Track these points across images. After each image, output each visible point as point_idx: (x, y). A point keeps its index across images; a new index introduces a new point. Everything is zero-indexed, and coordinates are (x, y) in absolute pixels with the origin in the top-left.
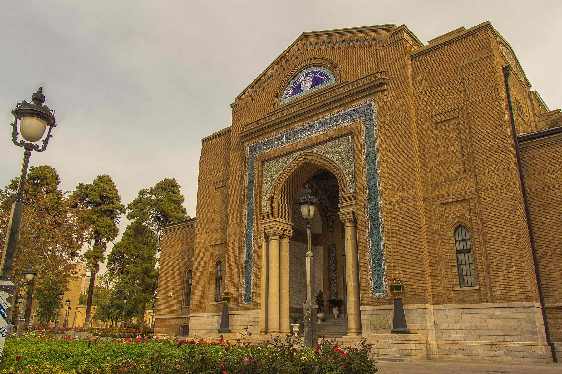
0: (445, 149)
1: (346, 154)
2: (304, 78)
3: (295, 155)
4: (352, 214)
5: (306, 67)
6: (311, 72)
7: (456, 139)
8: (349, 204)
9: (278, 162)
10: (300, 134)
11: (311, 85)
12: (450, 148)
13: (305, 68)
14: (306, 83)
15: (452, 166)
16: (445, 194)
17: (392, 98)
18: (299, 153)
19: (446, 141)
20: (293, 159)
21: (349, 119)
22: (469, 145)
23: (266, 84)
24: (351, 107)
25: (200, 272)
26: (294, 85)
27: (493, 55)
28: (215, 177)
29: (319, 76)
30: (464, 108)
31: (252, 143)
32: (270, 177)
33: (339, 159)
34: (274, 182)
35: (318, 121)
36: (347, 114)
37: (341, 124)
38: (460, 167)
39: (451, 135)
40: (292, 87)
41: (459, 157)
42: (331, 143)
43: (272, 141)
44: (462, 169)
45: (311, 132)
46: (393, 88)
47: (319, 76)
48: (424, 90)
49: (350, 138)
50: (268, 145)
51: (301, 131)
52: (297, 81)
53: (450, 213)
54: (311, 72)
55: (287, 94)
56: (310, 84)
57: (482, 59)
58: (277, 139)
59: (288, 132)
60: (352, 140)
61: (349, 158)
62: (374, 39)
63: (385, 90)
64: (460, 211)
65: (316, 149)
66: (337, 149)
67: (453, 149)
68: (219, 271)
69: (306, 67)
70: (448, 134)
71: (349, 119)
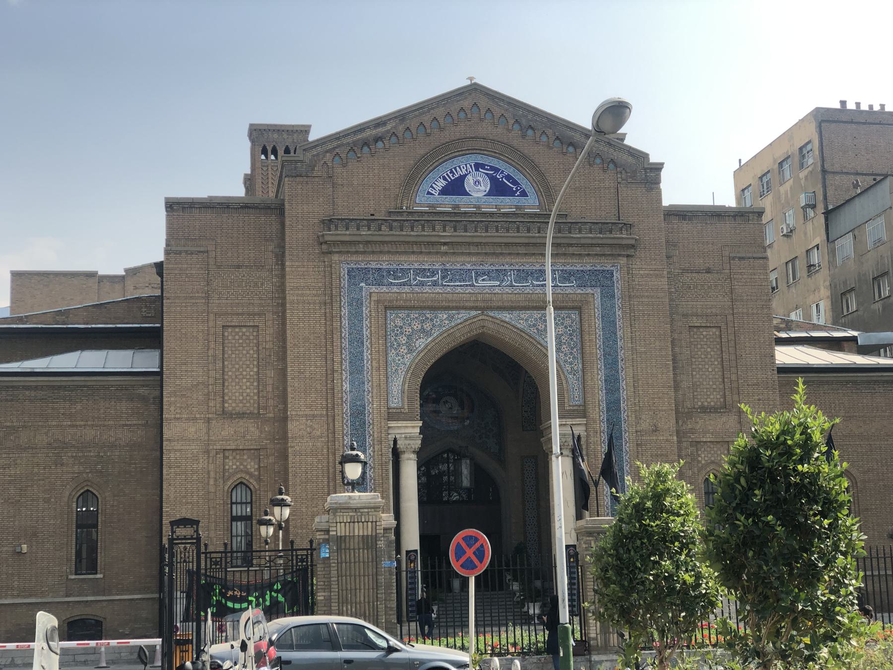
0: (700, 366)
1: (566, 340)
2: (470, 170)
3: (463, 315)
5: (478, 151)
6: (488, 166)
7: (716, 356)
9: (422, 317)
10: (476, 280)
11: (487, 190)
12: (707, 366)
13: (475, 151)
14: (477, 183)
15: (709, 393)
16: (699, 429)
17: (641, 272)
18: (473, 313)
19: (703, 356)
20: (459, 321)
21: (573, 283)
22: (733, 370)
23: (380, 144)
24: (579, 263)
25: (188, 503)
26: (447, 174)
27: (766, 258)
28: (219, 299)
29: (504, 179)
30: (730, 318)
31: (357, 262)
32: (404, 342)
34: (414, 354)
35: (512, 267)
37: (557, 286)
38: (718, 397)
39: (709, 350)
40: (445, 179)
41: (718, 383)
42: (539, 314)
43: (410, 272)
44: (722, 400)
45: (499, 283)
46: (643, 255)
47: (504, 179)
48: (677, 271)
49: (574, 315)
50: (399, 278)
51: (478, 275)
52: (455, 168)
53: (703, 456)
54: (488, 166)
55: (432, 186)
56: (486, 188)
57: (754, 258)
59: (448, 266)
60: (578, 319)
61: (572, 348)
62: (612, 161)
64: (716, 455)
65: (508, 316)
67: (710, 370)
68: (234, 503)
69: (478, 151)
70: (705, 346)
71: (573, 283)
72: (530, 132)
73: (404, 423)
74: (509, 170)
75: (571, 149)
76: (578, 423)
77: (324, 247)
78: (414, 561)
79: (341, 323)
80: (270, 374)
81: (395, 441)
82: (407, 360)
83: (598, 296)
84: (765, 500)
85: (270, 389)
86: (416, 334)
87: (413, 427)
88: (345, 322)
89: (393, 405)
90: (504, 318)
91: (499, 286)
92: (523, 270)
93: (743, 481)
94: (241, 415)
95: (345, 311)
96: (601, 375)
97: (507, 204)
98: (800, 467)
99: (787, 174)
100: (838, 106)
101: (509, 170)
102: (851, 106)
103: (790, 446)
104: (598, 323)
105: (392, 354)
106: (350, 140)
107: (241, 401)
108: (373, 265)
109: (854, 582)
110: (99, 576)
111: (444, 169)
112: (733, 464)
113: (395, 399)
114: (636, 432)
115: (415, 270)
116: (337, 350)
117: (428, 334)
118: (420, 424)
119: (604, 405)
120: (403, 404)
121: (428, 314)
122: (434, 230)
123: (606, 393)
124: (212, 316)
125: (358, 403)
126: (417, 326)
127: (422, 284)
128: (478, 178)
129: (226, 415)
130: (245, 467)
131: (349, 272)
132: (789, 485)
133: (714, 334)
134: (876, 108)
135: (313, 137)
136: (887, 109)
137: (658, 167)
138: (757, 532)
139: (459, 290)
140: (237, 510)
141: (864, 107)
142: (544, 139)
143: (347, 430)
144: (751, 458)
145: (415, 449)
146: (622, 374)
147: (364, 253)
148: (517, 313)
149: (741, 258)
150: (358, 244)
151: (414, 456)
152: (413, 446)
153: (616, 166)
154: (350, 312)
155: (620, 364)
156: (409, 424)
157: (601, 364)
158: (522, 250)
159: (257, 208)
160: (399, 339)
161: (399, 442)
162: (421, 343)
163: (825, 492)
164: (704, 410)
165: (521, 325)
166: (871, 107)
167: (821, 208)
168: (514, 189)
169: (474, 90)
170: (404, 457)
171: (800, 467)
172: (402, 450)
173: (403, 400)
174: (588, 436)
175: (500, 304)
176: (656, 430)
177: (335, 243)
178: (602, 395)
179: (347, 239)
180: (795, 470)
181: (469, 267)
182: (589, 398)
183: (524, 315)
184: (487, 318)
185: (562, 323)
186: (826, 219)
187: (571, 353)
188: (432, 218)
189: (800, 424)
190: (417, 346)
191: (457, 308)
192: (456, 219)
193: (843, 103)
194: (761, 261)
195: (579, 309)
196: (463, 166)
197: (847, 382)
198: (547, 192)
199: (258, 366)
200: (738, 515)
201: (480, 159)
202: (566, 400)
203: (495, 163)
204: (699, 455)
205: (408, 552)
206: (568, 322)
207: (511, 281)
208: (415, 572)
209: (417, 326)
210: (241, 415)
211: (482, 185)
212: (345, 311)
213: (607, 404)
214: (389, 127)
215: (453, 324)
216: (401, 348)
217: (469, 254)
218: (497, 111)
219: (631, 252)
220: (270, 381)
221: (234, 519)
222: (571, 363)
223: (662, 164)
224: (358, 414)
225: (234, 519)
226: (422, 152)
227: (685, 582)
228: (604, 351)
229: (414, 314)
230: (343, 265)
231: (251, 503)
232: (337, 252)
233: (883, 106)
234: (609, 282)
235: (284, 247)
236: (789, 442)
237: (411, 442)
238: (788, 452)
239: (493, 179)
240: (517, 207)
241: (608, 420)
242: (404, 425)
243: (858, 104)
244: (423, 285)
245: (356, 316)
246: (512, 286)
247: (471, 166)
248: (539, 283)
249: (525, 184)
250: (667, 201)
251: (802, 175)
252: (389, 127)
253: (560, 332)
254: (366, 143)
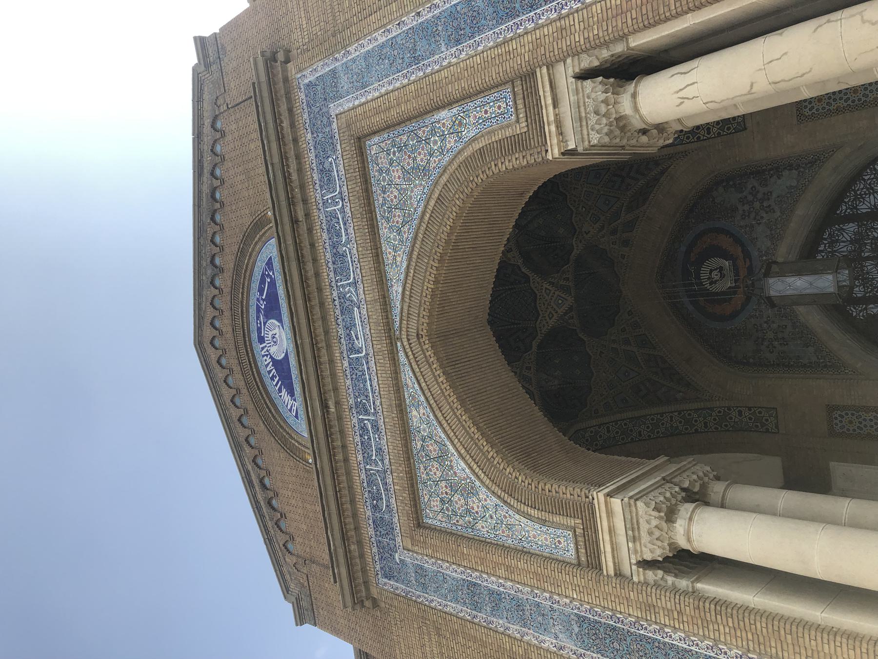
3: (407, 376)
4: (588, 83)
6: (257, 323)
8: (549, 101)
11: (278, 324)
20: (416, 386)
21: (331, 163)
33: (421, 184)
34: (478, 483)
37: (340, 193)
47: (264, 297)
51: (353, 349)
58: (366, 446)
60: (376, 139)
63: (288, 52)
66: (395, 197)
76: (548, 88)
79: (451, 614)
81: (645, 564)
82: (488, 501)
86: (447, 474)
87: (610, 513)
89: (572, 552)
90: (399, 297)
91: (359, 308)
92: (334, 263)
113: (559, 542)
120: (567, 528)
121: (416, 444)
123: (480, 31)
125: (576, 629)
126: (436, 471)
128: (270, 336)
131: (386, 577)
137: (201, 43)
139: (375, 384)
145: (660, 518)
150: (350, 551)
152: (654, 522)
156: (603, 524)
160: (459, 509)
161: (648, 557)
162: (460, 467)
165: (402, 260)
168: (269, 280)
172: (668, 548)
173: (558, 526)
174: (576, 53)
181: (346, 364)
182: (494, 74)
184: (404, 329)
190: (464, 475)
195: (359, 138)
201: (254, 336)
202: (509, 132)
207: (349, 284)
211: (274, 332)
213: (500, 21)
215: (422, 398)
216: (473, 508)
219: (281, 57)
222: (443, 137)
223: (195, 38)
228: (410, 65)
232: (368, 589)
234: (319, 88)
237: (644, 527)
242: (607, 537)
244: (381, 449)
246: (355, 283)
247: (263, 348)
248: (343, 230)
252: (250, 468)
253: (400, 172)
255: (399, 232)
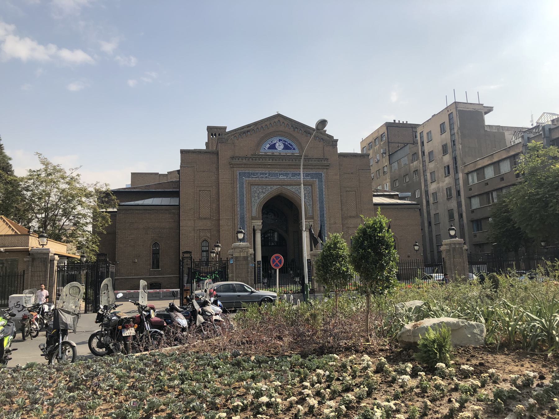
3: (275, 187)
18: (278, 187)
20: (274, 189)
23: (249, 133)
27: (370, 169)
31: (242, 170)
36: (309, 174)
40: (269, 144)
49: (310, 187)
68: (204, 246)
72: (296, 129)
73: (257, 221)
74: (289, 142)
75: (309, 135)
77: (231, 165)
78: (260, 264)
80: (214, 206)
81: (254, 226)
83: (317, 181)
84: (368, 245)
85: (214, 210)
87: (260, 222)
88: (238, 189)
93: (361, 239)
94: (205, 219)
95: (238, 186)
96: (318, 206)
97: (289, 152)
98: (379, 234)
99: (377, 143)
100: (393, 122)
101: (289, 142)
102: (397, 122)
103: (376, 228)
104: (317, 190)
105: (253, 199)
106: (239, 131)
107: (205, 214)
108: (247, 171)
109: (395, 270)
110: (160, 269)
111: (269, 141)
112: (358, 233)
114: (329, 224)
115: (260, 173)
116: (236, 198)
117: (264, 193)
118: (262, 221)
119: (319, 216)
122: (266, 160)
124: (196, 187)
126: (261, 190)
127: (262, 177)
129: (200, 218)
130: (206, 235)
132: (375, 240)
133: (354, 193)
134: (405, 122)
135: (227, 131)
136: (408, 123)
137: (337, 141)
138: (365, 255)
139: (274, 179)
140: (204, 249)
141: (401, 122)
142: (301, 132)
143: (239, 223)
144: (364, 232)
146: (325, 206)
147: (244, 167)
148: (291, 187)
149: (362, 169)
151: (260, 231)
153: (323, 140)
154: (240, 186)
155: (324, 203)
156: (258, 221)
157: (318, 203)
158: (293, 167)
159: (209, 153)
161: (255, 227)
162: (262, 196)
163: (386, 242)
164: (350, 217)
165: (293, 190)
166: (403, 122)
167: (387, 154)
169: (279, 116)
170: (256, 231)
171: (379, 234)
175: (287, 184)
176: (335, 223)
177: (235, 164)
178: (319, 212)
179: (239, 163)
180: (377, 235)
183: (294, 187)
185: (306, 190)
186: (389, 157)
187: (309, 199)
188: (266, 156)
189: (379, 221)
191: (273, 185)
192: (273, 157)
193: (395, 121)
194: (368, 171)
195: (311, 185)
196: (275, 140)
197: (395, 208)
198: (301, 149)
199: (210, 203)
200: (360, 249)
203: (285, 139)
204: (349, 231)
205: (258, 261)
206: (308, 189)
208: (260, 267)
209: (261, 190)
210: (205, 219)
212: (238, 186)
214: (252, 127)
217: (277, 168)
218: (286, 122)
219: (328, 167)
220: (214, 208)
221: (203, 251)
223: (338, 140)
224: (242, 219)
225: (203, 251)
226: (262, 136)
227: (343, 270)
229: (260, 187)
230: (237, 171)
231: (208, 246)
233: (407, 122)
235: (219, 165)
236: (376, 227)
238: (375, 230)
239: (284, 144)
240: (292, 153)
241: (320, 220)
243: (399, 121)
245: (242, 187)
249: (295, 146)
250: (339, 152)
251: (382, 143)
252: (252, 127)
254: (244, 133)
255: (297, 190)
